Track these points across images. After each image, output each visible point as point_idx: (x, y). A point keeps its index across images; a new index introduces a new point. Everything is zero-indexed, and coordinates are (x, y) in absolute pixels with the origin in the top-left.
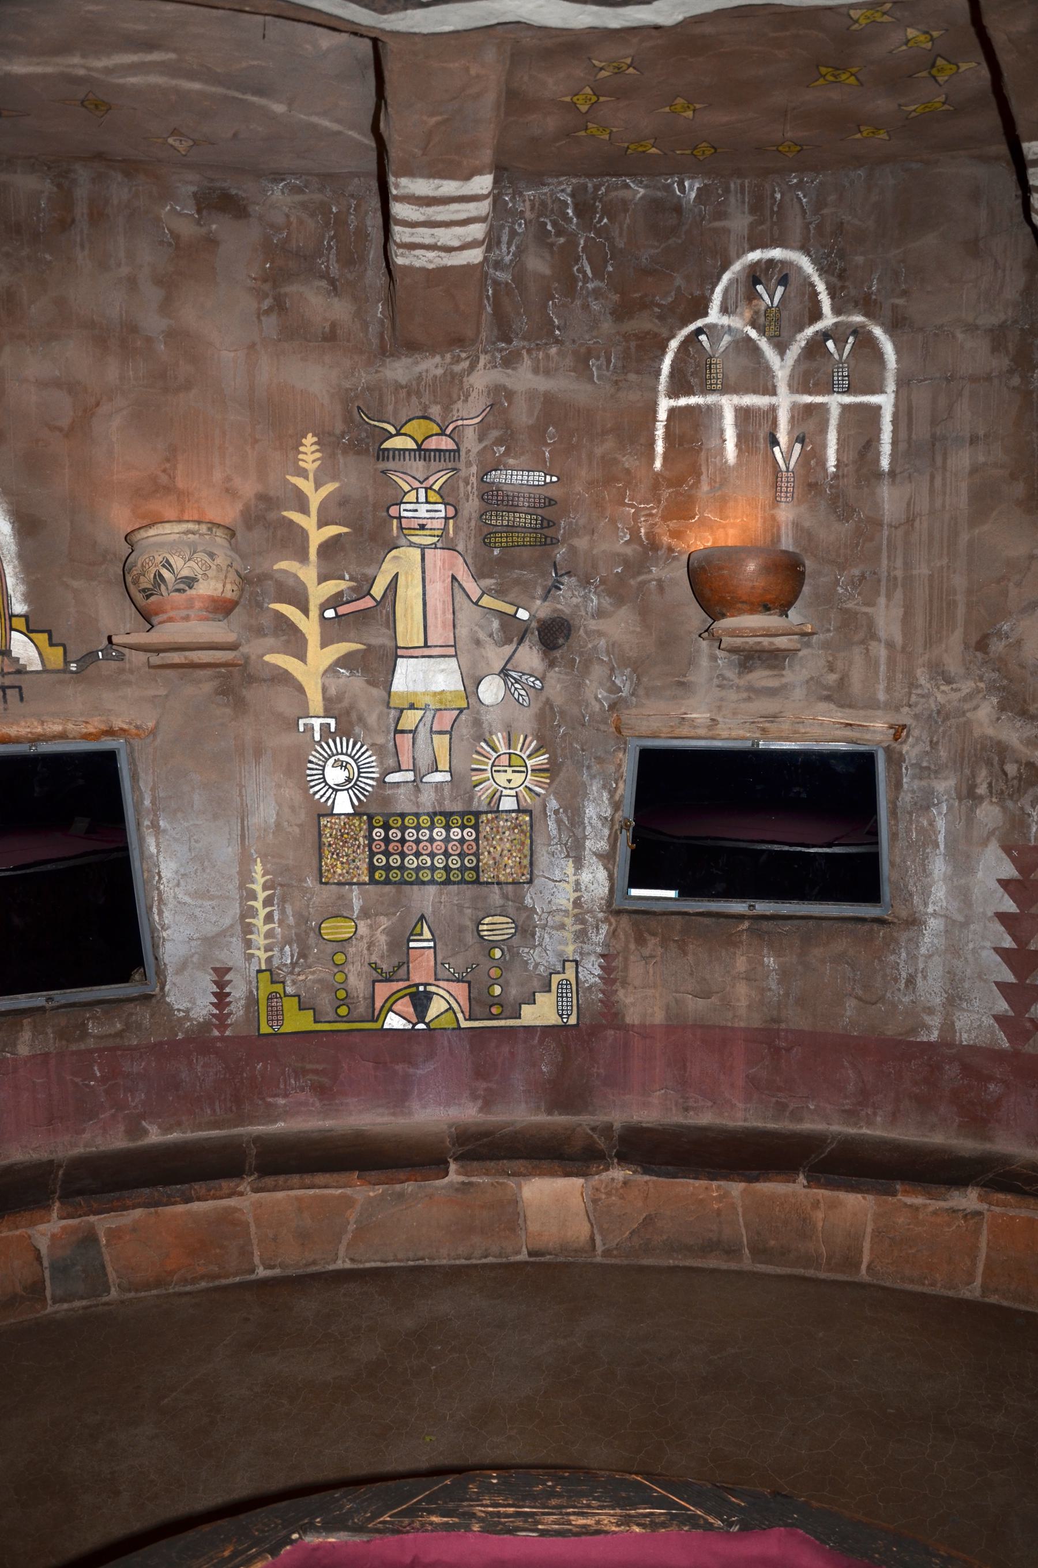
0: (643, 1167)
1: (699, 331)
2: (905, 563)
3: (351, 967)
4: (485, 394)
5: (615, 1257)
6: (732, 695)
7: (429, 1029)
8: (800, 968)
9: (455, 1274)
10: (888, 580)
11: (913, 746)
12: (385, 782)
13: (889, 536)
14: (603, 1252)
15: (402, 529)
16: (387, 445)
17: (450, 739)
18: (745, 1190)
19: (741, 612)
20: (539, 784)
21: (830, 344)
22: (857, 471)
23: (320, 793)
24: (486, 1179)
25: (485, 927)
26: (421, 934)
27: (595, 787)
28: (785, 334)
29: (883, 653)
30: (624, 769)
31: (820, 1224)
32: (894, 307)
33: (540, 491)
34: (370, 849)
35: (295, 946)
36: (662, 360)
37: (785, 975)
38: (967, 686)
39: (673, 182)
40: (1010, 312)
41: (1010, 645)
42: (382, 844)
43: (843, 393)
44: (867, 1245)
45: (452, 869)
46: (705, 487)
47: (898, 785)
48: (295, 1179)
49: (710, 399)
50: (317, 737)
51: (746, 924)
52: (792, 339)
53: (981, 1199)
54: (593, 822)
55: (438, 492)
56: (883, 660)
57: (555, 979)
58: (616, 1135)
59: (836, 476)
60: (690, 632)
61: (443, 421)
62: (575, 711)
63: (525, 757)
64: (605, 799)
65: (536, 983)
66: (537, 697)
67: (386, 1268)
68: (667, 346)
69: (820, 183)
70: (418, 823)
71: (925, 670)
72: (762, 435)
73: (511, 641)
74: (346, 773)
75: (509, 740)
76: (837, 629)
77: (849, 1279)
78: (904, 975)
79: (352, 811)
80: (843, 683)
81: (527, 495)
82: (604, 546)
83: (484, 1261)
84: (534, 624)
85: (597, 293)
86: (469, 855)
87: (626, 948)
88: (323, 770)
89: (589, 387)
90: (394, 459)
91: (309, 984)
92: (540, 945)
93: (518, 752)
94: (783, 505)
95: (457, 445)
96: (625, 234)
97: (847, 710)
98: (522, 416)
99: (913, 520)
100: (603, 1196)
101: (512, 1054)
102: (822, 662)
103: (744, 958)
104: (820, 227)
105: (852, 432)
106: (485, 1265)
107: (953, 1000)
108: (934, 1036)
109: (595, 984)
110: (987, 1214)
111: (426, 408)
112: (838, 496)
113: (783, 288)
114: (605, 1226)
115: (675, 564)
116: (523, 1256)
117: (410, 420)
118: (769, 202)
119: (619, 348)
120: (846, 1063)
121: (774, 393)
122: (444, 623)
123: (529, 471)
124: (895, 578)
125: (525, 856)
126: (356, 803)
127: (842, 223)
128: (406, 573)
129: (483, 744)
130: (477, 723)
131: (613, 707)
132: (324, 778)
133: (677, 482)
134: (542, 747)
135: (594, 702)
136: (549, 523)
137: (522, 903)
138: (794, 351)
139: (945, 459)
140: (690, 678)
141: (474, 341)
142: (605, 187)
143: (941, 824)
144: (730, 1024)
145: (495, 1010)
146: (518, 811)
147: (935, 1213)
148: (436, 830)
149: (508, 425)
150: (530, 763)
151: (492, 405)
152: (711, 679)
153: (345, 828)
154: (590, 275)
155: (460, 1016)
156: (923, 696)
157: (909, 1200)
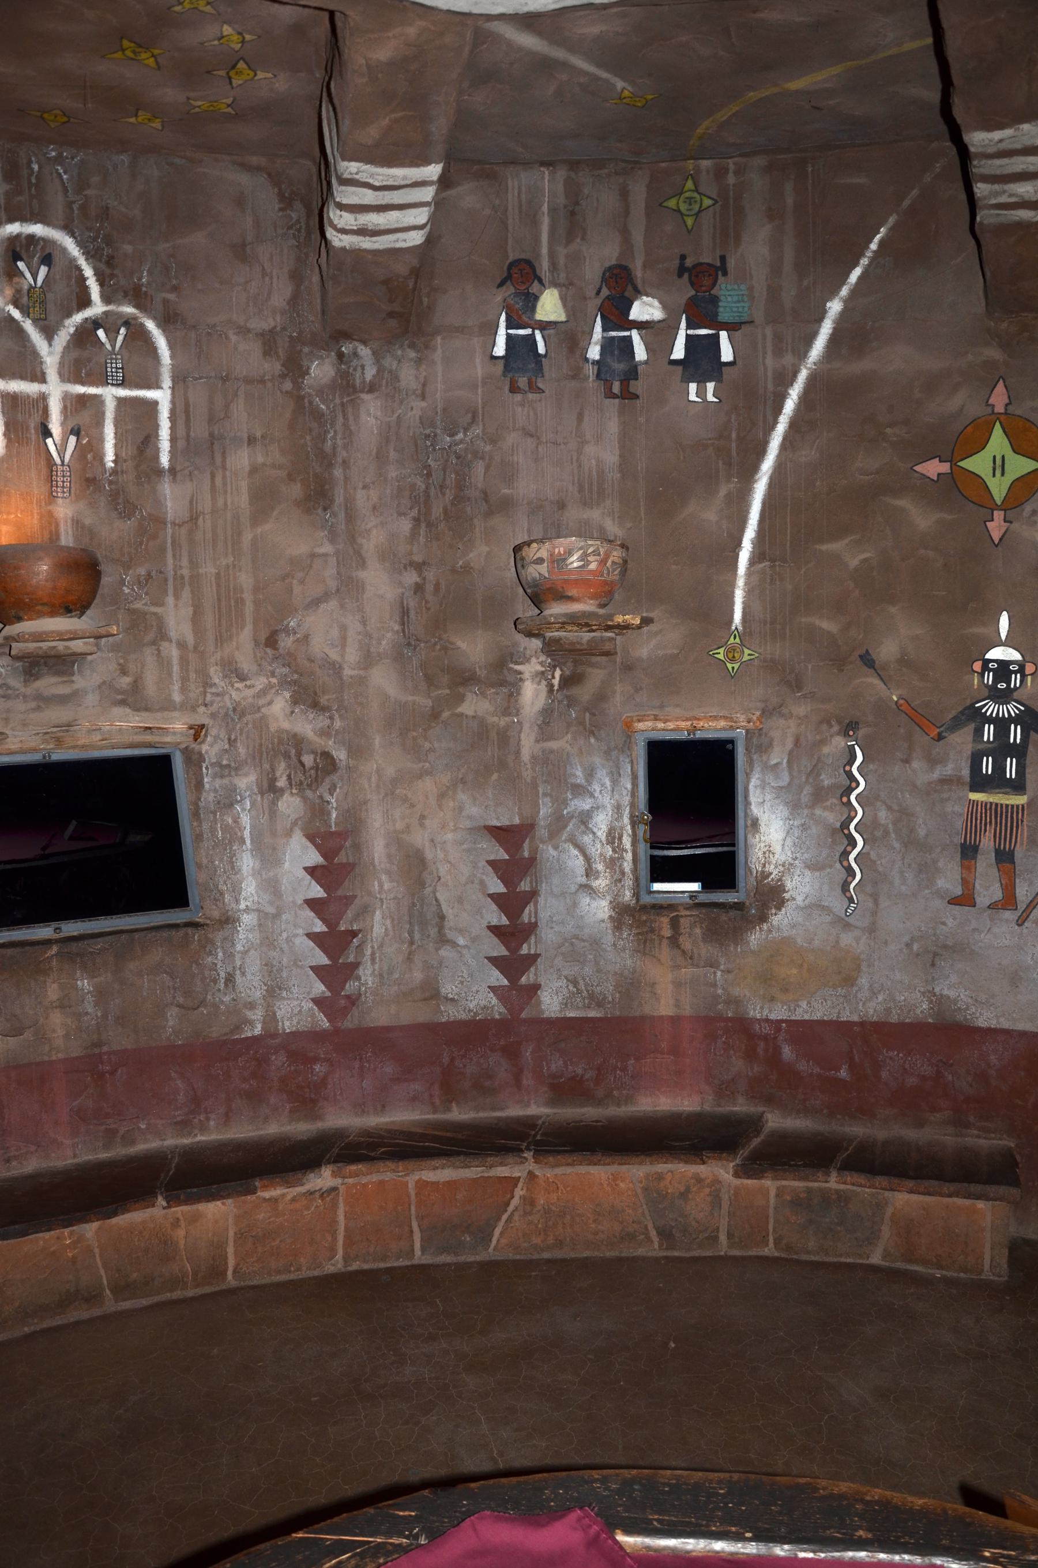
2: (191, 562)
6: (19, 706)
8: (116, 986)
10: (175, 579)
11: (211, 746)
13: (173, 534)
19: (40, 615)
21: (101, 333)
22: (137, 467)
28: (52, 318)
29: (175, 653)
31: (182, 1243)
32: (166, 302)
37: (101, 995)
38: (260, 682)
40: (278, 318)
43: (118, 385)
44: (230, 1250)
47: (199, 785)
51: (55, 949)
53: (334, 1175)
56: (175, 661)
59: (114, 472)
71: (218, 668)
72: (32, 425)
77: (217, 1289)
78: (223, 974)
80: (136, 686)
94: (60, 501)
99: (197, 519)
102: (113, 666)
103: (55, 986)
104: (83, 208)
107: (274, 990)
110: (342, 1189)
112: (118, 493)
113: (46, 269)
118: (25, 172)
120: (173, 1074)
121: (42, 379)
124: (182, 577)
127: (107, 208)
138: (62, 338)
143: (246, 820)
144: (46, 1058)
147: (294, 1200)
156: (218, 695)
157: (267, 1194)
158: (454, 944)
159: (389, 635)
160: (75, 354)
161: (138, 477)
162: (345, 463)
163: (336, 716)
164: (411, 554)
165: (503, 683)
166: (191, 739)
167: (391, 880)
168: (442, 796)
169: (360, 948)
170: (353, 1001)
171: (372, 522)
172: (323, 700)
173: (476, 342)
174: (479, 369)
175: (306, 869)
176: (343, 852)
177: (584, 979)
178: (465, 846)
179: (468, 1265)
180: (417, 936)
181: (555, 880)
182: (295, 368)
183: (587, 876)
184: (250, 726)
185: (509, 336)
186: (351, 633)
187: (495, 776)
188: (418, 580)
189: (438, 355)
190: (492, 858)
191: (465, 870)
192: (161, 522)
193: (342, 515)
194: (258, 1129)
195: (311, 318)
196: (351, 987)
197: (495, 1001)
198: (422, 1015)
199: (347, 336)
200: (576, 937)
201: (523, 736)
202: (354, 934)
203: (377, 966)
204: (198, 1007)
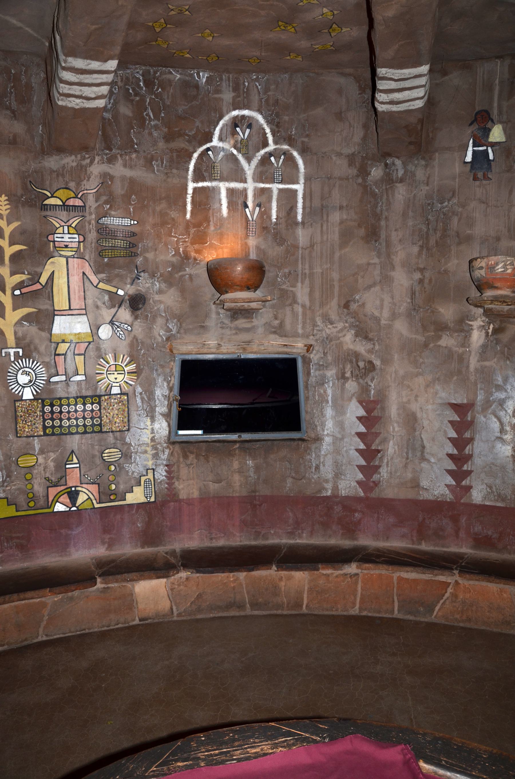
0: (196, 570)
1: (208, 149)
2: (310, 266)
3: (35, 480)
4: (99, 177)
5: (183, 616)
6: (228, 332)
7: (78, 510)
8: (264, 465)
9: (103, 635)
10: (302, 275)
11: (315, 355)
12: (50, 382)
13: (302, 253)
14: (177, 614)
15: (55, 247)
16: (46, 202)
17: (84, 358)
18: (246, 576)
20: (131, 380)
21: (272, 159)
22: (286, 221)
23: (15, 389)
24: (116, 585)
25: (106, 455)
26: (72, 461)
27: (160, 380)
28: (251, 153)
29: (300, 310)
30: (174, 370)
31: (283, 589)
32: (303, 142)
33: (128, 228)
34: (43, 418)
35: (4, 471)
36: (189, 163)
37: (257, 469)
38: (340, 325)
39: (194, 72)
40: (356, 148)
41: (359, 306)
42: (50, 414)
43: (279, 183)
44: (305, 596)
45: (87, 426)
46: (212, 228)
47: (308, 374)
48: (15, 596)
49: (214, 184)
50: (12, 359)
51: (238, 445)
52: (254, 156)
53: (358, 567)
54: (159, 398)
55: (75, 228)
56: (300, 314)
57: (143, 479)
58: (178, 555)
59: (276, 224)
60: (206, 301)
61: (77, 191)
62: (148, 341)
63: (123, 366)
64: (165, 386)
65: (133, 482)
66: (129, 335)
67: (66, 637)
68: (192, 156)
69: (267, 79)
70: (69, 402)
71: (320, 318)
73: (115, 306)
74: (29, 377)
75: (115, 357)
76: (278, 298)
79: (32, 398)
80: (281, 325)
81: (121, 230)
82: (162, 258)
83: (117, 627)
84: (127, 297)
85: (156, 127)
86: (96, 418)
87: (178, 461)
88: (16, 377)
89: (152, 175)
90: (50, 210)
91: (13, 491)
92: (135, 462)
93: (120, 364)
94: (251, 238)
95: (84, 203)
96: (170, 97)
97: (284, 338)
98: (119, 189)
99: (313, 246)
100: (176, 587)
101: (122, 519)
102: (271, 315)
103: (237, 462)
104: (267, 101)
105: (284, 202)
106: (117, 629)
107: (338, 475)
108: (329, 493)
109: (163, 480)
110: (361, 575)
111: (67, 183)
112: (277, 234)
114: (178, 601)
115: (198, 266)
116: (137, 622)
117: (58, 189)
119: (168, 156)
121: (245, 181)
122: (79, 297)
123: (122, 218)
124: (305, 274)
125: (125, 417)
126: (35, 393)
127: (278, 100)
128: (59, 271)
129: (102, 360)
130: (98, 349)
131: (168, 339)
132: (17, 381)
133: (198, 225)
134: (132, 360)
135: (158, 337)
136: (133, 245)
137: (125, 441)
138: (255, 161)
139: (328, 217)
140: (207, 324)
141: (94, 149)
142: (160, 72)
143: (329, 392)
144: (231, 495)
145: (112, 497)
146: (121, 394)
147: (337, 576)
148: (78, 406)
149: (111, 194)
150: (126, 369)
151: (102, 183)
152: (217, 324)
153: (29, 407)
154: (152, 117)
155: (94, 502)
156: (319, 331)
157: (325, 572)
158: (429, 461)
159: (405, 304)
160: (260, 169)
161: (287, 226)
162: (387, 218)
163: (377, 344)
164: (417, 263)
165: (462, 331)
166: (305, 351)
167: (399, 426)
168: (427, 386)
169: (381, 459)
170: (376, 484)
171: (399, 247)
172: (370, 336)
173: (456, 155)
174: (457, 168)
175: (357, 417)
176: (376, 411)
177: (496, 487)
178: (438, 412)
179: (421, 623)
180: (410, 455)
181: (484, 434)
182: (364, 172)
183: (501, 432)
184: (334, 346)
185: (474, 151)
186: (386, 303)
187: (455, 378)
188: (421, 277)
189: (436, 163)
190: (451, 419)
191: (437, 425)
192: (296, 247)
193: (384, 244)
194: (325, 541)
195: (372, 147)
196: (375, 477)
197: (448, 492)
198: (409, 494)
199: (389, 155)
200: (493, 464)
201: (471, 358)
202: (379, 451)
203: (389, 468)
204: (301, 479)
